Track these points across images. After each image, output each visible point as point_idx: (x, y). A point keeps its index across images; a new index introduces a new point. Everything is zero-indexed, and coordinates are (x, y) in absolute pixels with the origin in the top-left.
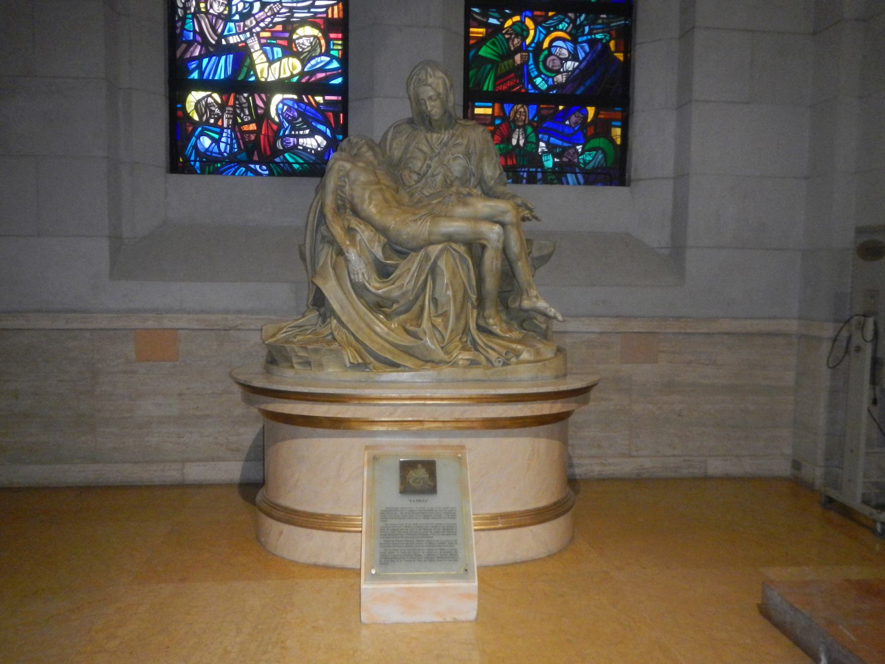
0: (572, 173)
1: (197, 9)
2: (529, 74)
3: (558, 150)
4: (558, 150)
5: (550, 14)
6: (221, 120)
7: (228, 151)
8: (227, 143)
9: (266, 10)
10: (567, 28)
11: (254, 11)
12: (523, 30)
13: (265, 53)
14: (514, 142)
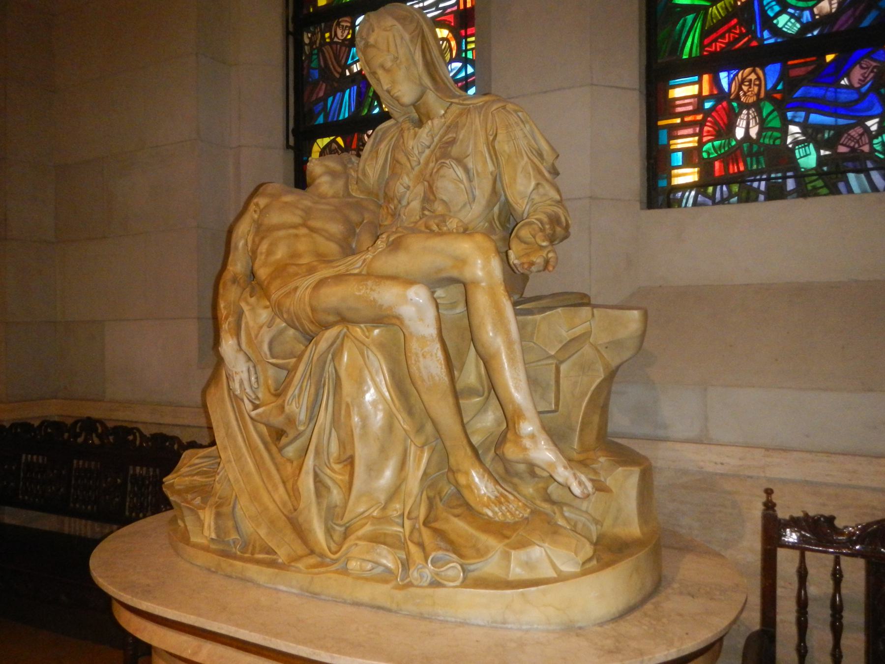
0: (857, 171)
2: (763, 12)
3: (826, 135)
4: (826, 135)
14: (740, 133)
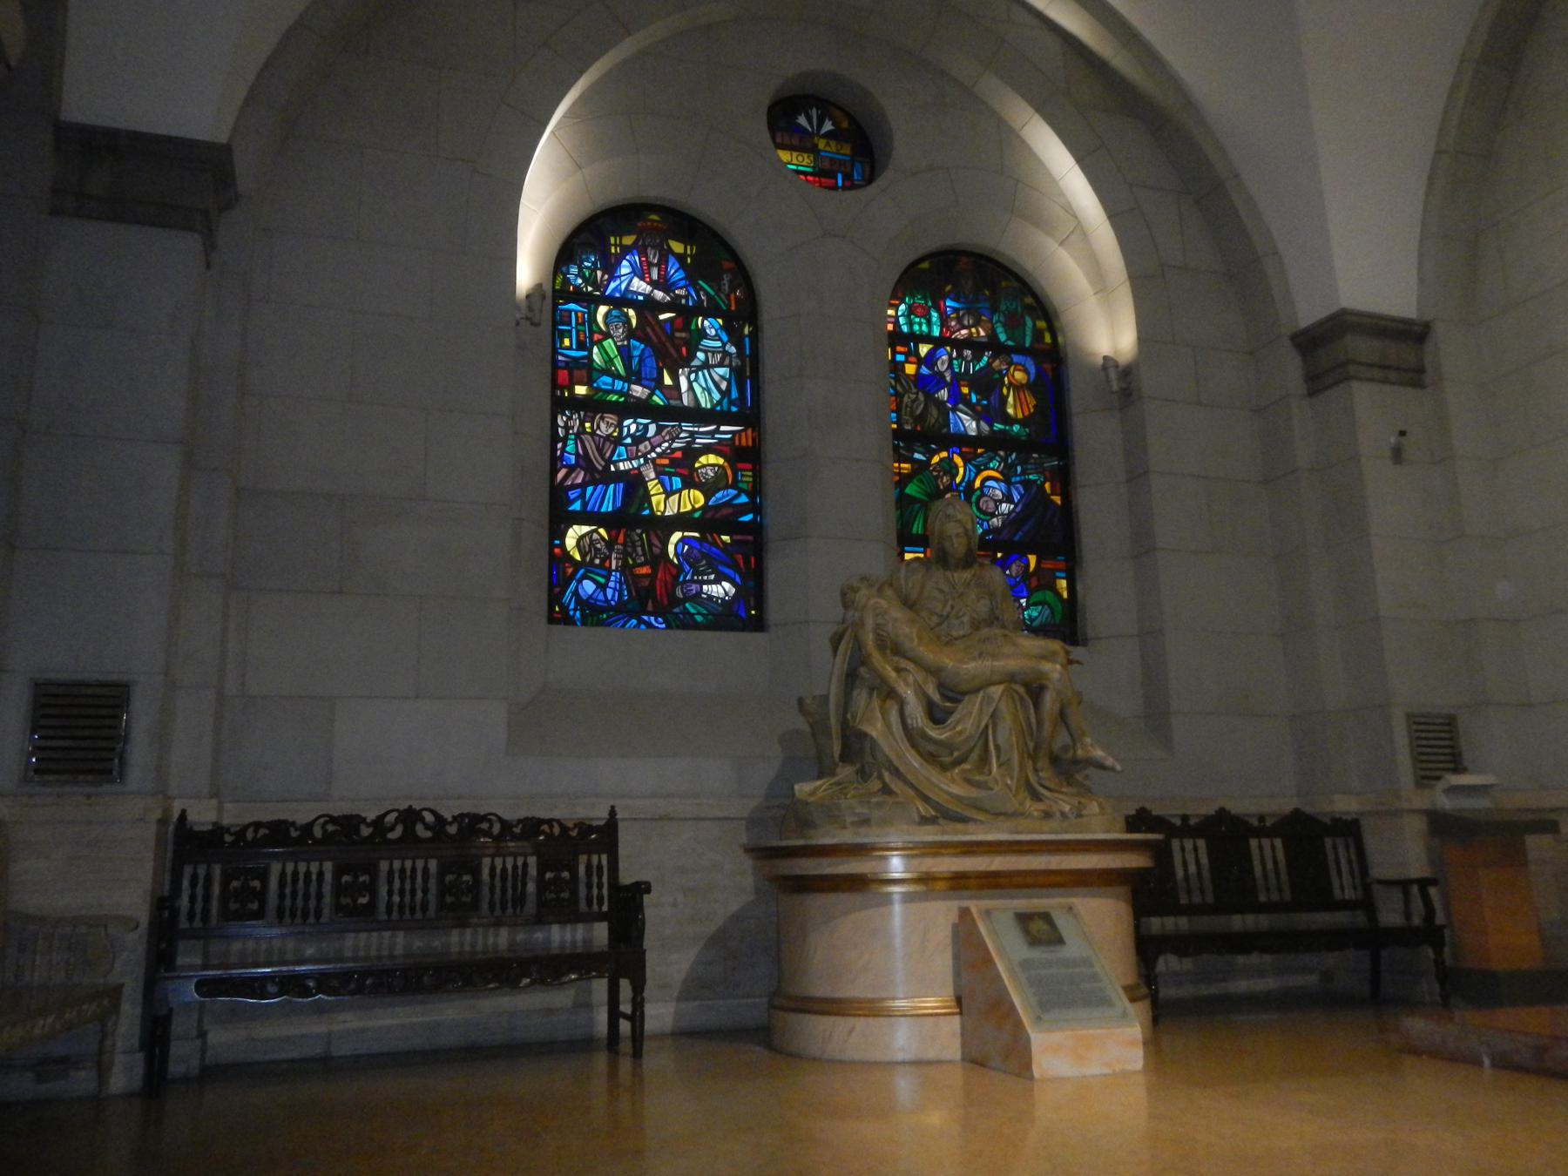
5: (979, 451)
6: (608, 561)
8: (615, 589)
9: (663, 434)
10: (998, 467)
11: (649, 435)
12: (951, 467)
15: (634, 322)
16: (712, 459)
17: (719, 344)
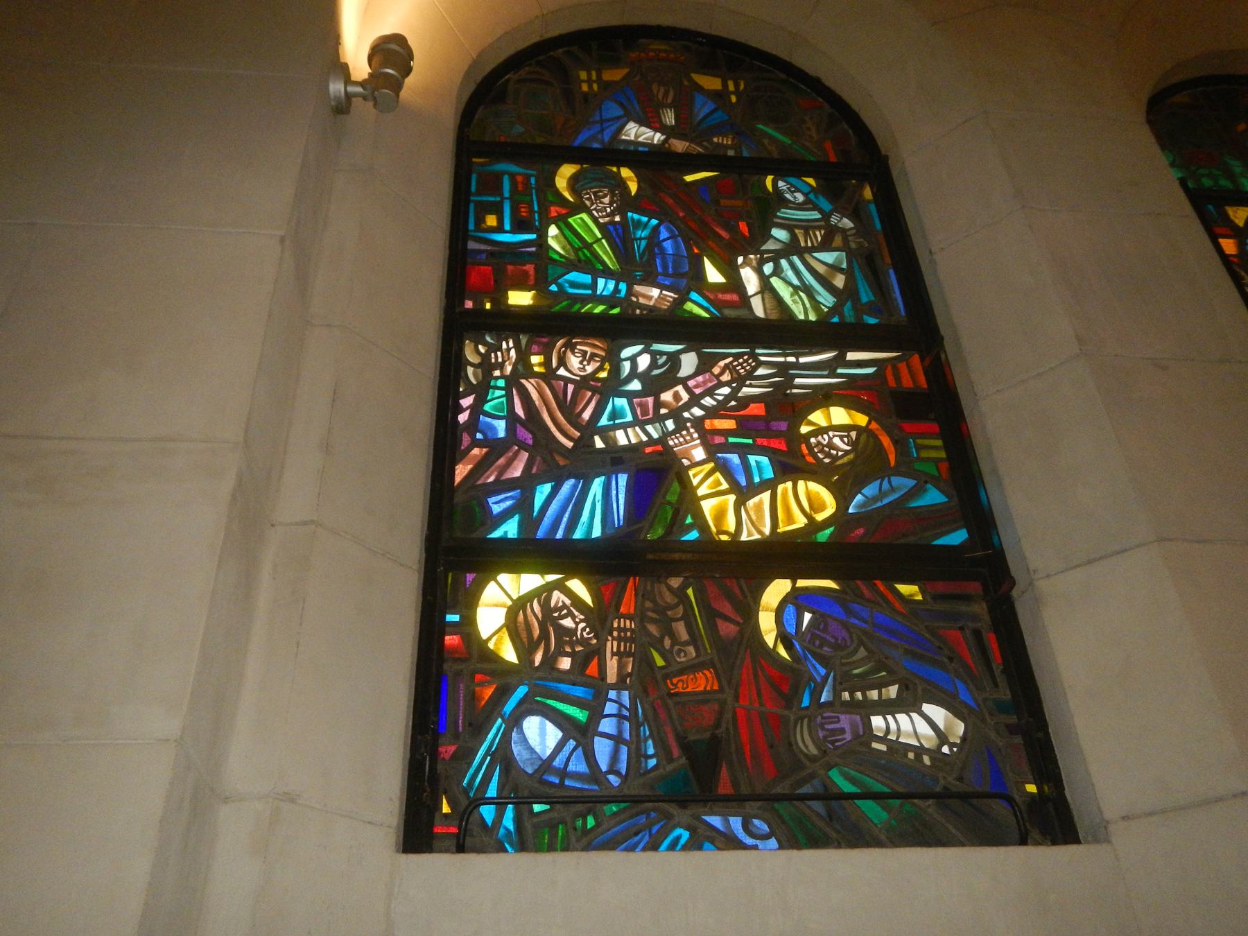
1: (520, 367)
6: (595, 661)
7: (623, 767)
8: (617, 739)
9: (716, 370)
13: (724, 469)
15: (633, 187)
16: (839, 415)
17: (815, 215)
